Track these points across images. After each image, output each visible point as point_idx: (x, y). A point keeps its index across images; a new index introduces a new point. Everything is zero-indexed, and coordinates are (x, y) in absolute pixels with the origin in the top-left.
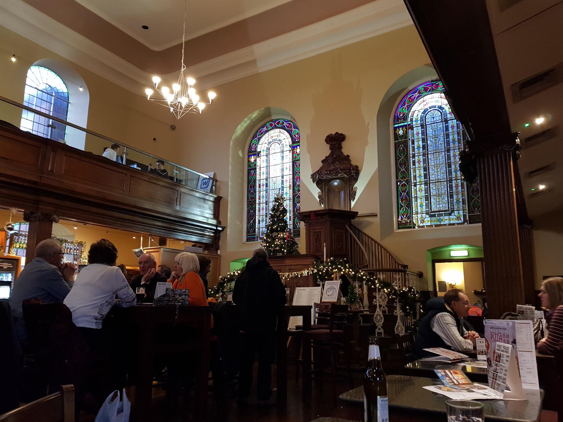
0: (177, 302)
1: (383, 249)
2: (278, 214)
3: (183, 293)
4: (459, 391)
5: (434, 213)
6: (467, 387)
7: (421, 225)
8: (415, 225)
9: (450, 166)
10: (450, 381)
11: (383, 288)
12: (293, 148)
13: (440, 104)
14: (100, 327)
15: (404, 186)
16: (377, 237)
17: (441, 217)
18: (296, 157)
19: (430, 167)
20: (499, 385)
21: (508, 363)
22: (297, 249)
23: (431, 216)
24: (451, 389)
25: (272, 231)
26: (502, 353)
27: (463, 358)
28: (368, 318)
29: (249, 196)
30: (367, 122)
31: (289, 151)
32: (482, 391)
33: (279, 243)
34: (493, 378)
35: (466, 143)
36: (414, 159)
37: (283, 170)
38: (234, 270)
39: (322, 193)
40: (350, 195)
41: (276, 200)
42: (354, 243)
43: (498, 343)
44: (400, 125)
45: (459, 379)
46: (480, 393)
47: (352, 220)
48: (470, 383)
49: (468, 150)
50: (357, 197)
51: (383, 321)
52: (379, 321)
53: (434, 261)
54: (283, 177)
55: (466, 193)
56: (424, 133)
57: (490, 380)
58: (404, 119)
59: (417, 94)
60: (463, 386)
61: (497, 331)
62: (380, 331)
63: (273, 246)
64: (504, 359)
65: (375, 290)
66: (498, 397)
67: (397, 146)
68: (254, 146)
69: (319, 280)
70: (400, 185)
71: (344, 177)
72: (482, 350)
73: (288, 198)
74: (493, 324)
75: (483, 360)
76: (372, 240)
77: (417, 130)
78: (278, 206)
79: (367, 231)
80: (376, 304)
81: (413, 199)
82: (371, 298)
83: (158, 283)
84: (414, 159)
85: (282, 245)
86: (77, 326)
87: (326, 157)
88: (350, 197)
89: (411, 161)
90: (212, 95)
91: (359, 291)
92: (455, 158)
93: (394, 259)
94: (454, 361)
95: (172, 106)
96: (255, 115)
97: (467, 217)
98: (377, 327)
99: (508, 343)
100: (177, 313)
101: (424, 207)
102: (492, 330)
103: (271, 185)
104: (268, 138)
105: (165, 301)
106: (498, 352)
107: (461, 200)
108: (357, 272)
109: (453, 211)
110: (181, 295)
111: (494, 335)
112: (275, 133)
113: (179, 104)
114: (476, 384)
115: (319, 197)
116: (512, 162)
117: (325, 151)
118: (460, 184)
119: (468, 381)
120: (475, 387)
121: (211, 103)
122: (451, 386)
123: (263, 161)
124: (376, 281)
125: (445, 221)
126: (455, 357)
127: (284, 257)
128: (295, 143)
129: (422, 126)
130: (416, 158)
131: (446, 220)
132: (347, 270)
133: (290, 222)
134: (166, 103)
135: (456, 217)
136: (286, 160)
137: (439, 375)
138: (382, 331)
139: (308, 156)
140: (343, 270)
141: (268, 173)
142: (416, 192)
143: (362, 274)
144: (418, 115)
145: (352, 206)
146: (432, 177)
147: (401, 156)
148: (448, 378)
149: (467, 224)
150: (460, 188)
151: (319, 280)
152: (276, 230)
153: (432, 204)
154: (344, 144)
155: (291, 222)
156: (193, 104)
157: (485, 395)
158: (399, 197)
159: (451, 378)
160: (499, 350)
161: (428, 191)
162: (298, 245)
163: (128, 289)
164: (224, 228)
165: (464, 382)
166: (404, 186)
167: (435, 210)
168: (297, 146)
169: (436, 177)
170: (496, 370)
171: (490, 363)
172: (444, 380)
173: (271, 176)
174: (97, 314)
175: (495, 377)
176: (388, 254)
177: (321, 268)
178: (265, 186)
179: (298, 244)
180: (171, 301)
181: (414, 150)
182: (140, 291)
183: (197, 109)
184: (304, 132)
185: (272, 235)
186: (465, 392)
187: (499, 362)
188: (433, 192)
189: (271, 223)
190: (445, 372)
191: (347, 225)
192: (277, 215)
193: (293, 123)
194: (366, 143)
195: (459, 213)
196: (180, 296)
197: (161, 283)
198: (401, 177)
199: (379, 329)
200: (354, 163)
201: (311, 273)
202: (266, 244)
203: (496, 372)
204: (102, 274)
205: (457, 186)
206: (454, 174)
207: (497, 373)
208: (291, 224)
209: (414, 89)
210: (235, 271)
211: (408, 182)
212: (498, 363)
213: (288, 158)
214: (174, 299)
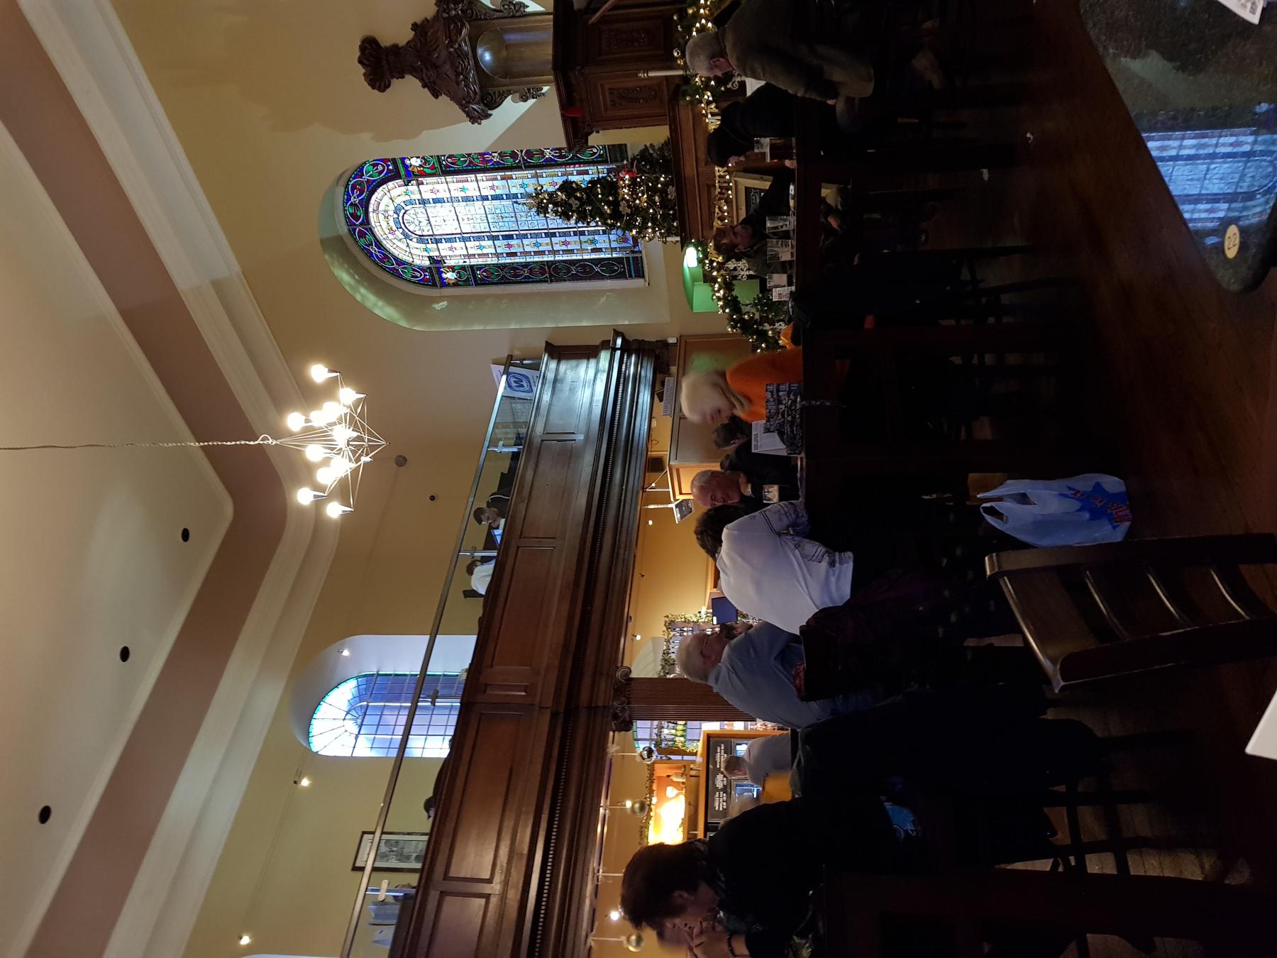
0: (796, 407)
2: (575, 203)
3: (775, 396)
12: (410, 176)
14: (849, 555)
18: (433, 168)
22: (656, 148)
25: (616, 215)
31: (420, 186)
33: (645, 196)
37: (467, 199)
38: (713, 299)
39: (515, 92)
40: (513, 17)
41: (541, 209)
54: (485, 198)
69: (729, 86)
73: (534, 181)
78: (556, 204)
83: (753, 451)
85: (648, 189)
86: (849, 597)
88: (518, 14)
90: (319, 373)
95: (358, 460)
96: (345, 277)
100: (818, 403)
103: (507, 226)
104: (395, 241)
105: (792, 431)
112: (381, 224)
113: (351, 443)
115: (524, 98)
117: (408, 88)
127: (679, 180)
128: (397, 171)
133: (590, 172)
134: (355, 472)
141: (478, 237)
145: (539, 9)
151: (729, 86)
152: (615, 205)
154: (386, 40)
155: (592, 169)
156: (346, 415)
162: (648, 145)
163: (770, 510)
168: (406, 167)
173: (483, 227)
174: (824, 565)
177: (701, 81)
178: (511, 242)
179: (645, 145)
180: (794, 418)
185: (628, 215)
191: (591, 18)
192: (578, 206)
193: (349, 180)
196: (780, 402)
197: (753, 443)
208: (596, 171)
210: (714, 297)
214: (788, 412)
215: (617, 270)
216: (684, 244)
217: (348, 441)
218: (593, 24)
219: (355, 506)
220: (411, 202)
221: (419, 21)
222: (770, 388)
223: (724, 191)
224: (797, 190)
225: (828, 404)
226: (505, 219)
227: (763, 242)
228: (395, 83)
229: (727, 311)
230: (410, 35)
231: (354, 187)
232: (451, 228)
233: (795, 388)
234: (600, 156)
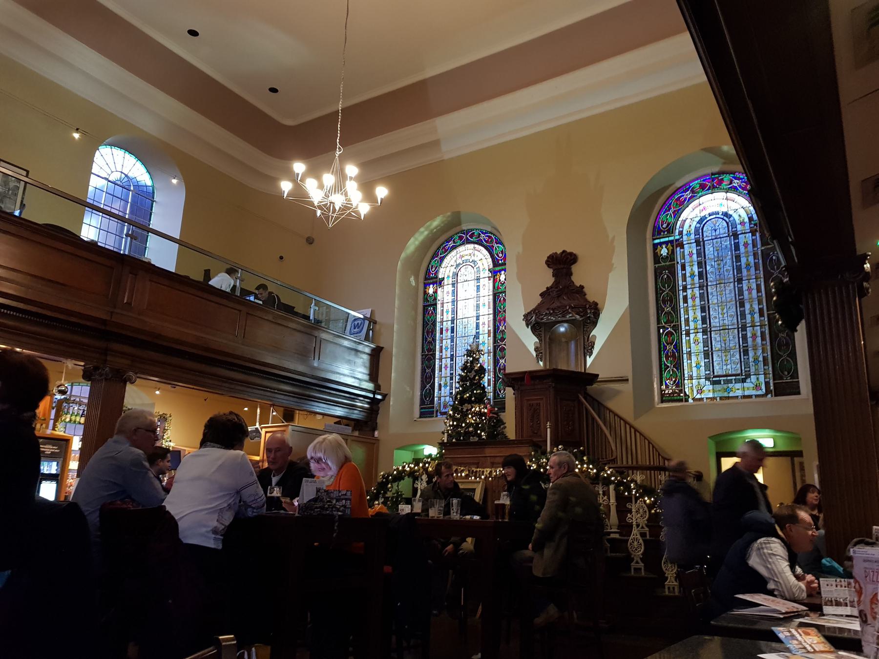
0: (334, 511)
1: (638, 434)
3: (342, 497)
5: (718, 379)
7: (698, 396)
8: (689, 397)
9: (742, 305)
10: (801, 646)
11: (642, 496)
12: (494, 273)
13: (725, 210)
14: (220, 547)
15: (670, 335)
17: (730, 385)
18: (498, 288)
19: (710, 306)
23: (714, 383)
25: (462, 401)
27: (800, 610)
28: (620, 545)
29: (425, 346)
30: (611, 236)
31: (488, 278)
33: (473, 422)
35: (784, 269)
36: (685, 294)
37: (478, 306)
38: (404, 463)
39: (540, 344)
41: (469, 353)
42: (593, 424)
44: (662, 240)
47: (587, 387)
48: (832, 650)
49: (788, 279)
50: (595, 351)
51: (642, 550)
52: (636, 550)
54: (478, 318)
55: (769, 348)
56: (701, 253)
58: (668, 231)
59: (688, 194)
62: (638, 566)
63: (463, 425)
65: (629, 499)
67: (657, 273)
68: (433, 269)
71: (575, 319)
72: (831, 598)
73: (486, 351)
74: (869, 554)
76: (621, 418)
77: (690, 248)
78: (472, 362)
79: (611, 405)
80: (632, 522)
81: (685, 356)
82: (623, 511)
83: (304, 479)
84: (685, 294)
85: (477, 424)
87: (547, 288)
88: (586, 351)
89: (681, 297)
90: (382, 192)
91: (603, 501)
92: (750, 293)
93: (656, 450)
95: (320, 207)
96: (436, 223)
97: (772, 384)
98: (633, 559)
100: (336, 528)
101: (703, 368)
102: (866, 565)
103: (460, 330)
104: (455, 258)
105: (317, 508)
107: (761, 359)
108: (601, 469)
109: (748, 376)
110: (340, 499)
112: (467, 250)
113: (332, 204)
115: (536, 350)
116: (857, 299)
117: (546, 279)
118: (759, 334)
121: (381, 203)
122: (804, 655)
123: (448, 293)
124: (632, 485)
125: (737, 391)
126: (788, 608)
127: (481, 444)
128: (498, 265)
129: (698, 242)
130: (689, 292)
131: (737, 390)
132: (585, 466)
134: (312, 204)
136: (483, 292)
137: (781, 636)
138: (641, 565)
139: (519, 286)
140: (579, 466)
141: (455, 311)
142: (690, 344)
143: (609, 472)
144: (690, 226)
145: (588, 364)
146: (715, 322)
147: (665, 287)
148: (795, 642)
149: (772, 396)
150: (759, 340)
152: (468, 401)
153: (715, 364)
154: (575, 268)
156: (352, 205)
158: (662, 352)
161: (707, 343)
162: (506, 425)
163: (258, 487)
164: (385, 396)
165: (823, 649)
166: (670, 335)
167: (720, 373)
168: (500, 271)
169: (721, 322)
171: (864, 619)
172: (790, 644)
173: (460, 315)
174: (215, 524)
176: (647, 442)
177: (543, 463)
178: (449, 331)
179: (505, 423)
180: (327, 509)
181: (684, 279)
182: (275, 492)
183: (357, 213)
184: (513, 250)
185: (462, 409)
188: (716, 346)
189: (461, 389)
190: (790, 632)
191: (582, 395)
193: (494, 235)
194: (610, 267)
195: (758, 379)
196: (338, 500)
197: (310, 479)
198: (665, 320)
199: (637, 562)
200: (590, 298)
202: (453, 423)
204: (220, 462)
205: (754, 336)
206: (748, 317)
208: (490, 391)
209: (685, 185)
211: (677, 328)
213: (487, 288)
214: (331, 505)
215: (426, 399)
216: (441, 445)
217: (333, 203)
218: (578, 397)
219: (287, 200)
221: (585, 290)
222: (349, 494)
223: (474, 474)
224: (476, 521)
225: (335, 535)
226: (464, 329)
227: (443, 497)
228: (550, 272)
230: (578, 283)
231: (490, 237)
232: (461, 295)
233: (347, 512)
234: (499, 395)
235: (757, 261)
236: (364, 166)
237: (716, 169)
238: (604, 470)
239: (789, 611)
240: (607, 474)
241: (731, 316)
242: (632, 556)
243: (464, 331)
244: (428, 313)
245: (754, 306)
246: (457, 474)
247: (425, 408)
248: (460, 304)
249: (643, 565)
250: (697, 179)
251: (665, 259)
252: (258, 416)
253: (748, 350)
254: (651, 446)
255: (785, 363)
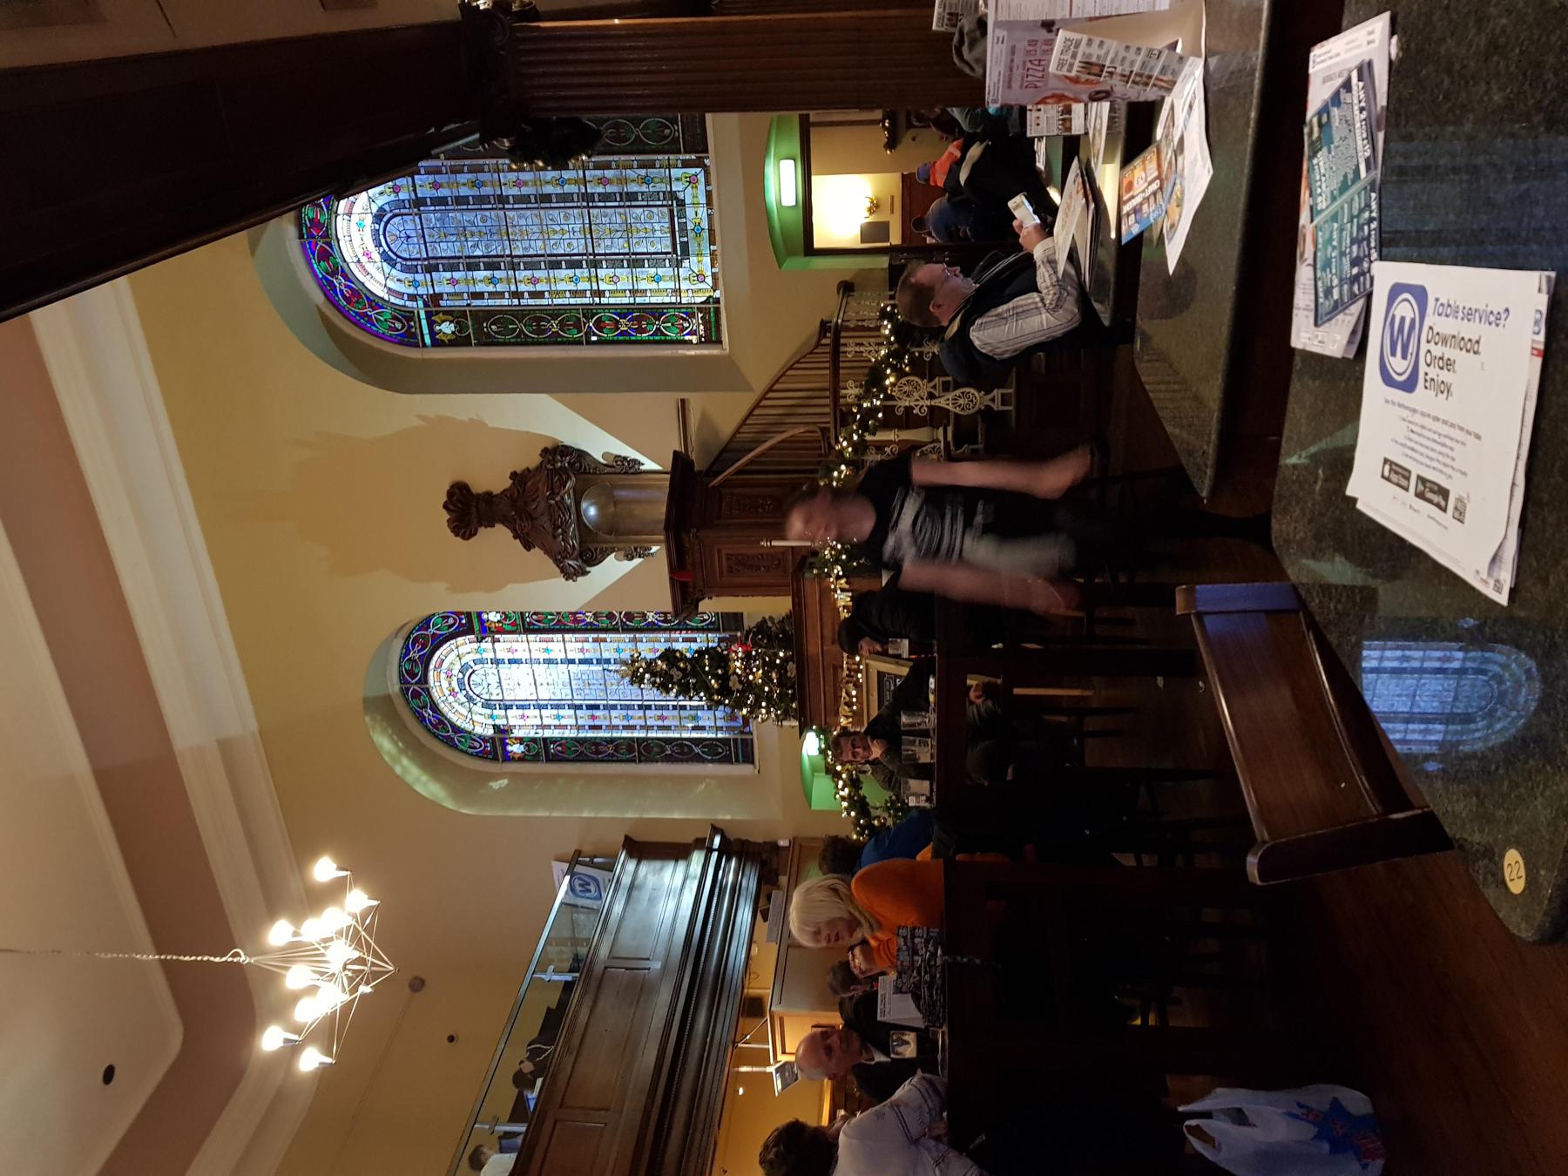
0: (936, 962)
1: (776, 387)
2: (677, 674)
3: (909, 944)
4: (1182, 176)
5: (678, 246)
6: (1167, 154)
7: (709, 280)
9: (546, 198)
11: (884, 389)
12: (485, 631)
13: (369, 219)
15: (602, 325)
16: (744, 402)
18: (513, 624)
19: (548, 252)
20: (1164, 70)
21: (1108, 42)
22: (776, 621)
23: (686, 253)
24: (1174, 196)
25: (725, 690)
26: (1079, 58)
27: (1079, 171)
30: (417, 423)
32: (1180, 116)
33: (760, 672)
34: (1147, 84)
36: (526, 295)
37: (549, 662)
39: (619, 550)
40: (626, 473)
41: (636, 679)
43: (1052, 68)
44: (426, 331)
45: (1146, 177)
46: (1186, 121)
47: (697, 468)
48: (1155, 149)
49: (505, 140)
50: (632, 454)
51: (972, 391)
52: (972, 401)
53: (809, 249)
54: (572, 662)
55: (623, 158)
57: (1150, 94)
59: (339, 282)
60: (1165, 166)
61: (1018, 73)
62: (998, 400)
64: (1095, 53)
65: (888, 410)
66: (1199, 72)
67: (487, 341)
70: (598, 336)
73: (631, 645)
75: (1085, 119)
76: (750, 414)
77: (442, 282)
78: (654, 674)
79: (726, 425)
81: (638, 300)
82: (909, 420)
83: (879, 1018)
84: (526, 295)
87: (515, 537)
88: (632, 471)
89: (531, 302)
92: (525, 183)
93: (804, 357)
94: (1090, 197)
95: (354, 990)
96: (385, 743)
97: (688, 157)
99: (1051, 43)
100: (965, 960)
101: (661, 271)
102: (1016, 84)
104: (456, 705)
105: (931, 996)
106: (1075, 68)
107: (643, 172)
109: (672, 195)
111: (1030, 78)
112: (440, 685)
113: (349, 967)
114: (1159, 132)
116: (542, 24)
117: (497, 539)
118: (599, 173)
119: (1150, 155)
120: (1167, 136)
122: (1166, 199)
124: (865, 405)
125: (699, 216)
127: (800, 658)
128: (471, 625)
129: (431, 269)
130: (522, 288)
131: (696, 214)
133: (699, 640)
134: (346, 1007)
135: (690, 188)
137: (1136, 230)
138: (997, 393)
139: (511, 588)
144: (398, 280)
146: (578, 246)
147: (514, 330)
148: (1145, 207)
149: (708, 158)
150: (609, 173)
152: (724, 679)
153: (652, 250)
154: (478, 487)
155: (700, 636)
157: (1191, 107)
158: (633, 338)
159: (1144, 199)
160: (1071, 65)
161: (615, 261)
162: (767, 617)
164: (715, 830)
165: (1154, 165)
166: (602, 325)
167: (669, 242)
168: (482, 622)
169: (578, 235)
170: (1124, 76)
171: (1104, 95)
172: (1148, 217)
173: (565, 693)
175: (1145, 79)
176: (789, 373)
178: (597, 713)
179: (764, 618)
180: (933, 977)
181: (500, 295)
183: (364, 916)
184: (441, 600)
185: (738, 691)
186: (1184, 159)
187: (1104, 66)
188: (620, 246)
189: (702, 694)
190: (1128, 215)
194: (477, 425)
195: (677, 179)
196: (915, 952)
198: (575, 331)
199: (993, 400)
200: (533, 460)
201: (843, 581)
203: (1129, 77)
205: (603, 181)
206: (568, 189)
207: (1131, 72)
209: (322, 287)
211: (589, 311)
212: (1106, 69)
214: (925, 968)
216: (802, 730)
217: (345, 965)
218: (713, 487)
219: (338, 1057)
220: (481, 661)
224: (938, 683)
225: (978, 961)
228: (483, 532)
229: (853, 814)
230: (508, 483)
231: (416, 640)
232: (524, 692)
235: (466, 169)
236: (272, 913)
237: (292, 231)
238: (841, 452)
239: (1082, 192)
240: (848, 447)
241: (567, 217)
242: (983, 408)
243: (594, 687)
244: (562, 752)
245: (549, 178)
246: (853, 704)
247: (737, 755)
248: (544, 694)
249: (996, 391)
250: (310, 265)
251: (461, 327)
252: (756, 1069)
253: (627, 193)
254: (796, 366)
255: (649, 131)
